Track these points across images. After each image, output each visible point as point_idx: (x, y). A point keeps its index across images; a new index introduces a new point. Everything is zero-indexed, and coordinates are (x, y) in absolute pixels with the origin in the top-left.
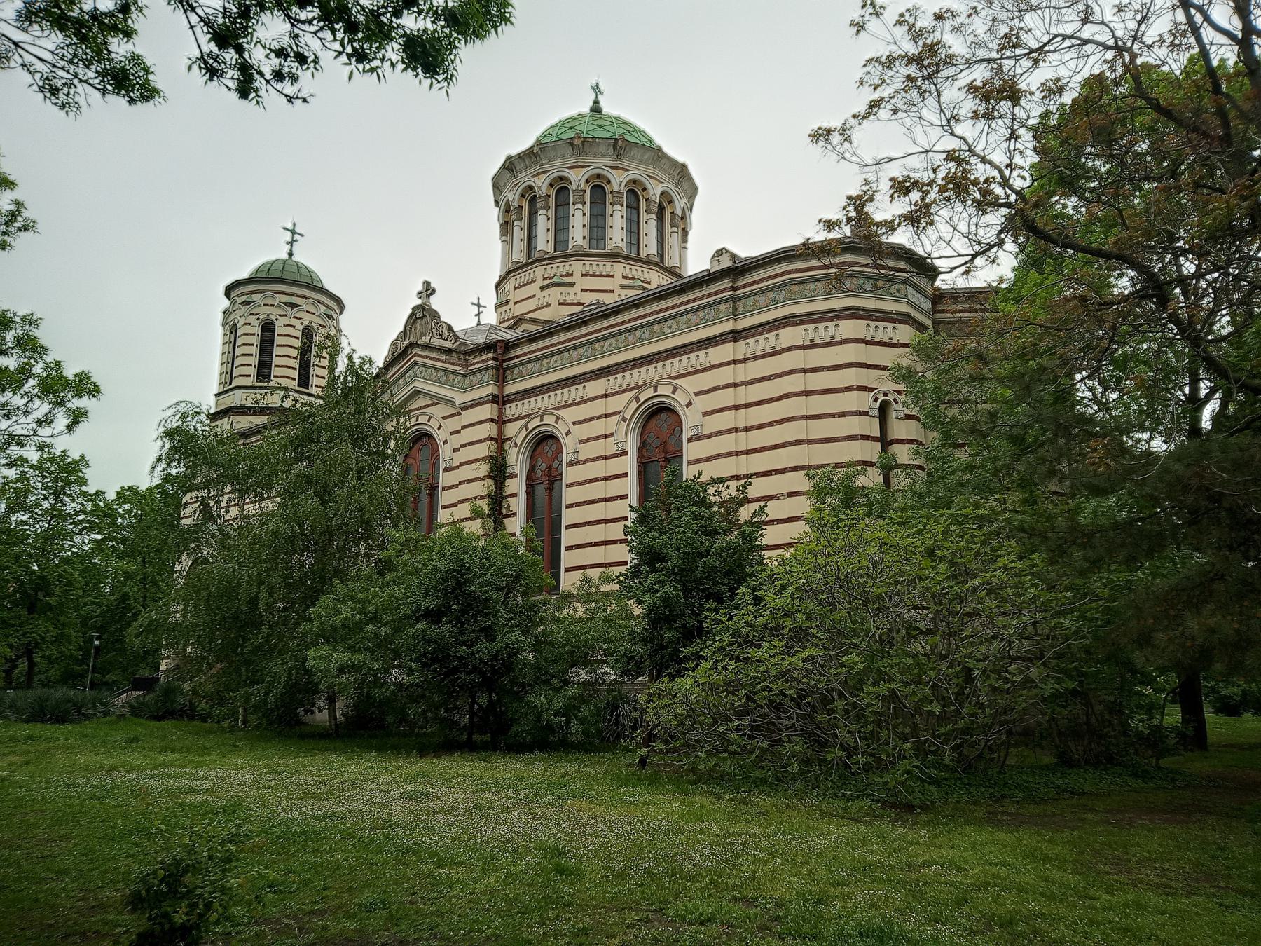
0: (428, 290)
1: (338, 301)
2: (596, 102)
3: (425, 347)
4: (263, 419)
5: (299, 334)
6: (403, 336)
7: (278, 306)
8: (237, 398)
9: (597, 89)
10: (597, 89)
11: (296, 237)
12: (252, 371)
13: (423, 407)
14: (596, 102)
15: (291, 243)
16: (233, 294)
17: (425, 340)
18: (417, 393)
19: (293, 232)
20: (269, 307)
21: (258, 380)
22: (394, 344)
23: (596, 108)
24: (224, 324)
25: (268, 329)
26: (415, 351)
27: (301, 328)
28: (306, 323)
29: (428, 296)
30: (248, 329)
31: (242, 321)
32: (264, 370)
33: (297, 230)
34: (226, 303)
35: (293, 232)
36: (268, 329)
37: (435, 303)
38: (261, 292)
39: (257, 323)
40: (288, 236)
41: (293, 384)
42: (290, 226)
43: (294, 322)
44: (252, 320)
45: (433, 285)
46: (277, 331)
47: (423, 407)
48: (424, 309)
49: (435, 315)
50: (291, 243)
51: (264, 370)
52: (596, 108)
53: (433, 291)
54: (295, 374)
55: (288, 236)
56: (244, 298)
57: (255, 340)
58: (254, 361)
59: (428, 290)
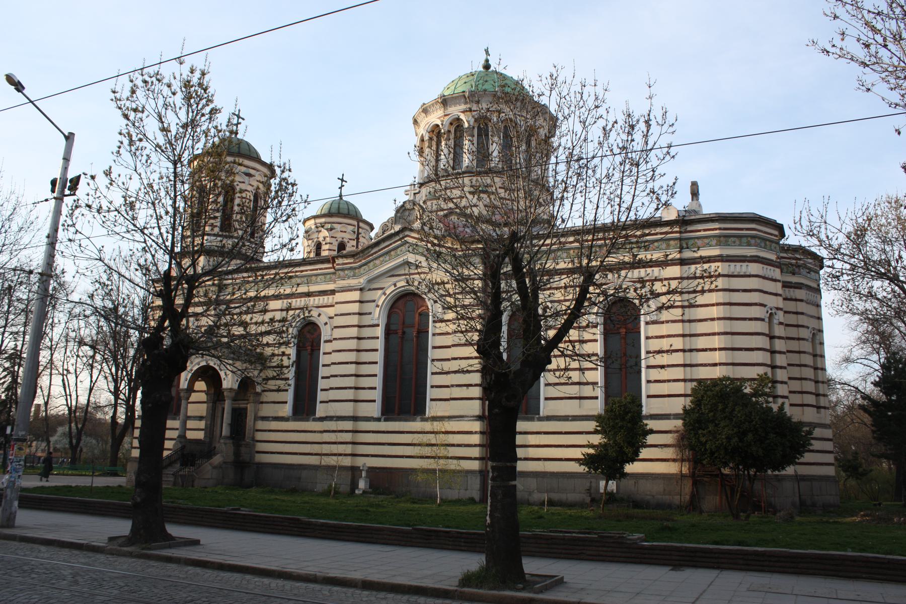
2: (487, 61)
6: (395, 220)
9: (487, 51)
10: (487, 51)
11: (240, 120)
14: (487, 61)
21: (221, 230)
23: (487, 66)
26: (407, 233)
33: (241, 115)
48: (414, 204)
52: (487, 66)
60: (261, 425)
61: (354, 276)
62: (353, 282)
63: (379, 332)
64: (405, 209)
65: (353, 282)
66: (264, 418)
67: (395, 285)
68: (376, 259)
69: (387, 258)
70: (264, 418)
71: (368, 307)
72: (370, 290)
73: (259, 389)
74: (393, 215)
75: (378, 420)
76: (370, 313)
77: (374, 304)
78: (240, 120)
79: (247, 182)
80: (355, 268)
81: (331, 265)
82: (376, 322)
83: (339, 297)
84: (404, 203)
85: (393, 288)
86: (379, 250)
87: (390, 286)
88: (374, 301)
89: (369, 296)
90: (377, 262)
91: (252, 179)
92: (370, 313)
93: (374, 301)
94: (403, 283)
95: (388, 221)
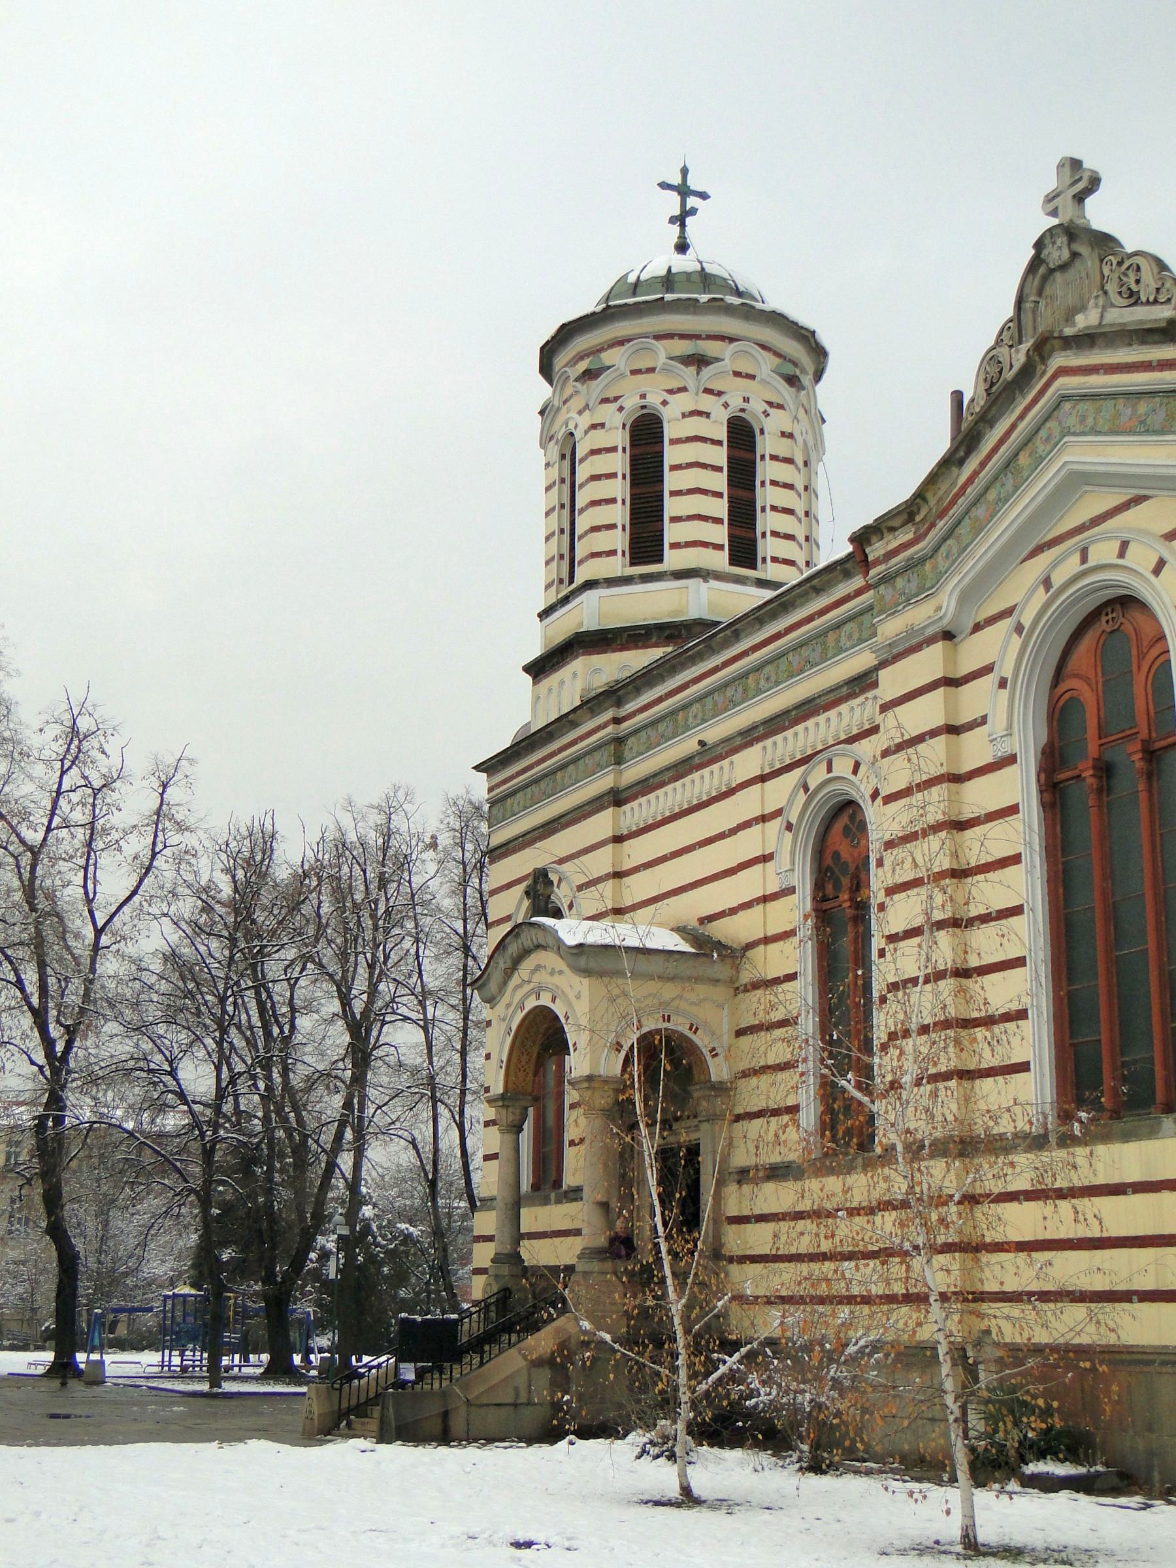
0: (1081, 182)
1: (807, 337)
3: (1088, 340)
4: (653, 654)
5: (722, 434)
6: (1015, 329)
7: (666, 370)
8: (591, 612)
11: (692, 202)
12: (619, 540)
13: (1097, 521)
15: (680, 220)
16: (560, 361)
17: (1083, 321)
18: (1079, 481)
19: (684, 191)
20: (644, 377)
22: (991, 359)
24: (546, 439)
25: (646, 434)
26: (1060, 360)
27: (721, 416)
28: (736, 402)
29: (1080, 198)
30: (600, 439)
31: (585, 421)
32: (646, 543)
33: (693, 183)
34: (543, 391)
35: (684, 191)
36: (646, 434)
37: (1099, 214)
38: (621, 342)
39: (618, 419)
40: (672, 203)
41: (720, 560)
42: (676, 180)
43: (707, 403)
44: (608, 413)
45: (1090, 163)
46: (669, 433)
47: (1097, 521)
49: (1104, 242)
50: (680, 220)
51: (646, 543)
53: (1094, 183)
54: (720, 534)
55: (672, 203)
56: (582, 366)
57: (619, 463)
58: (619, 514)
59: (1081, 182)
60: (736, 1201)
61: (922, 589)
62: (919, 615)
63: (1019, 785)
64: (1051, 271)
65: (919, 615)
66: (743, 1176)
67: (1047, 583)
68: (976, 502)
69: (1009, 481)
70: (743, 1176)
71: (976, 699)
72: (977, 628)
73: (718, 1070)
74: (1010, 312)
75: (1038, 1142)
76: (983, 721)
77: (990, 680)
78: (692, 202)
79: (691, 384)
80: (922, 561)
81: (858, 582)
82: (1003, 750)
83: (892, 682)
84: (1039, 245)
85: (1041, 596)
86: (983, 465)
87: (1032, 592)
88: (988, 669)
89: (976, 650)
90: (980, 512)
91: (707, 371)
92: (983, 721)
93: (988, 669)
94: (1072, 565)
95: (999, 342)
